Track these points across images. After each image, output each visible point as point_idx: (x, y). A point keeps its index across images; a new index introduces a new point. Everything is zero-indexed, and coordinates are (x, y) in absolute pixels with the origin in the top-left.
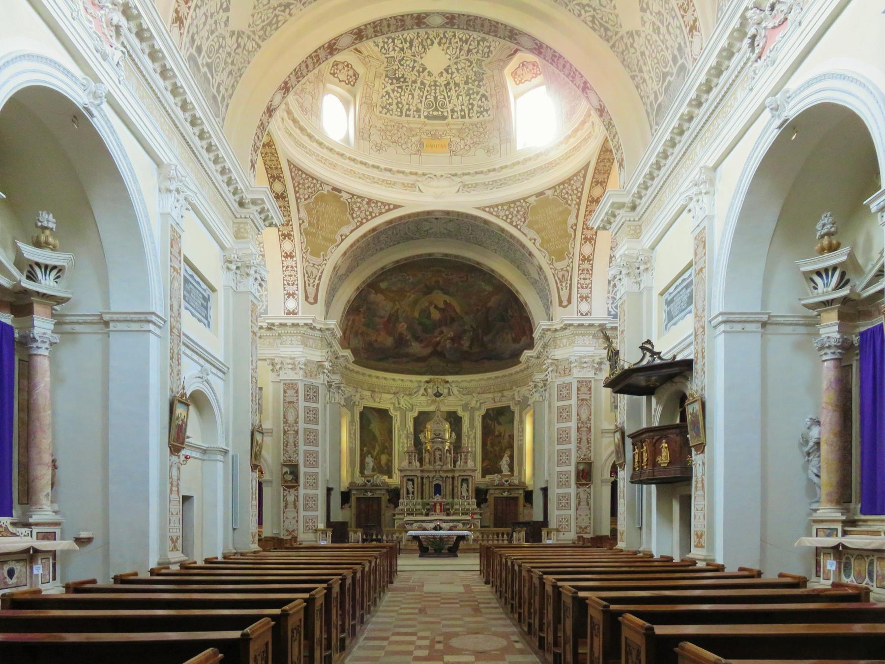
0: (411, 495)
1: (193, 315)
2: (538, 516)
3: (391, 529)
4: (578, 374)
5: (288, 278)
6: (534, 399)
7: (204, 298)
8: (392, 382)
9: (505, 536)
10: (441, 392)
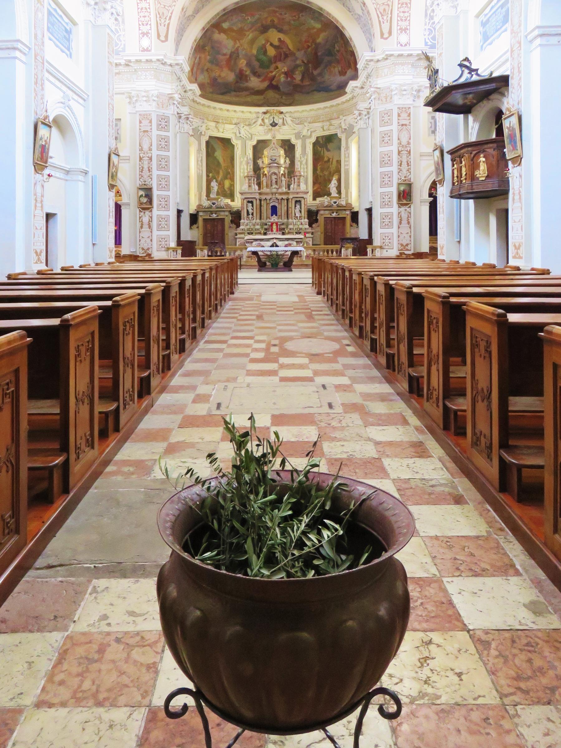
0: (251, 216)
1: (57, 46)
2: (364, 235)
3: (234, 247)
4: (398, 101)
6: (358, 127)
7: (66, 30)
8: (234, 113)
9: (334, 253)
10: (276, 122)
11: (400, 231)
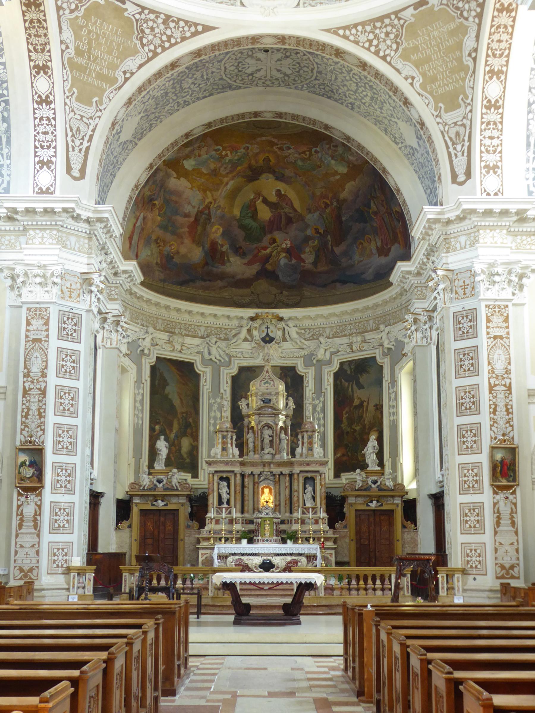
5: (41, 137)
11: (499, 538)
